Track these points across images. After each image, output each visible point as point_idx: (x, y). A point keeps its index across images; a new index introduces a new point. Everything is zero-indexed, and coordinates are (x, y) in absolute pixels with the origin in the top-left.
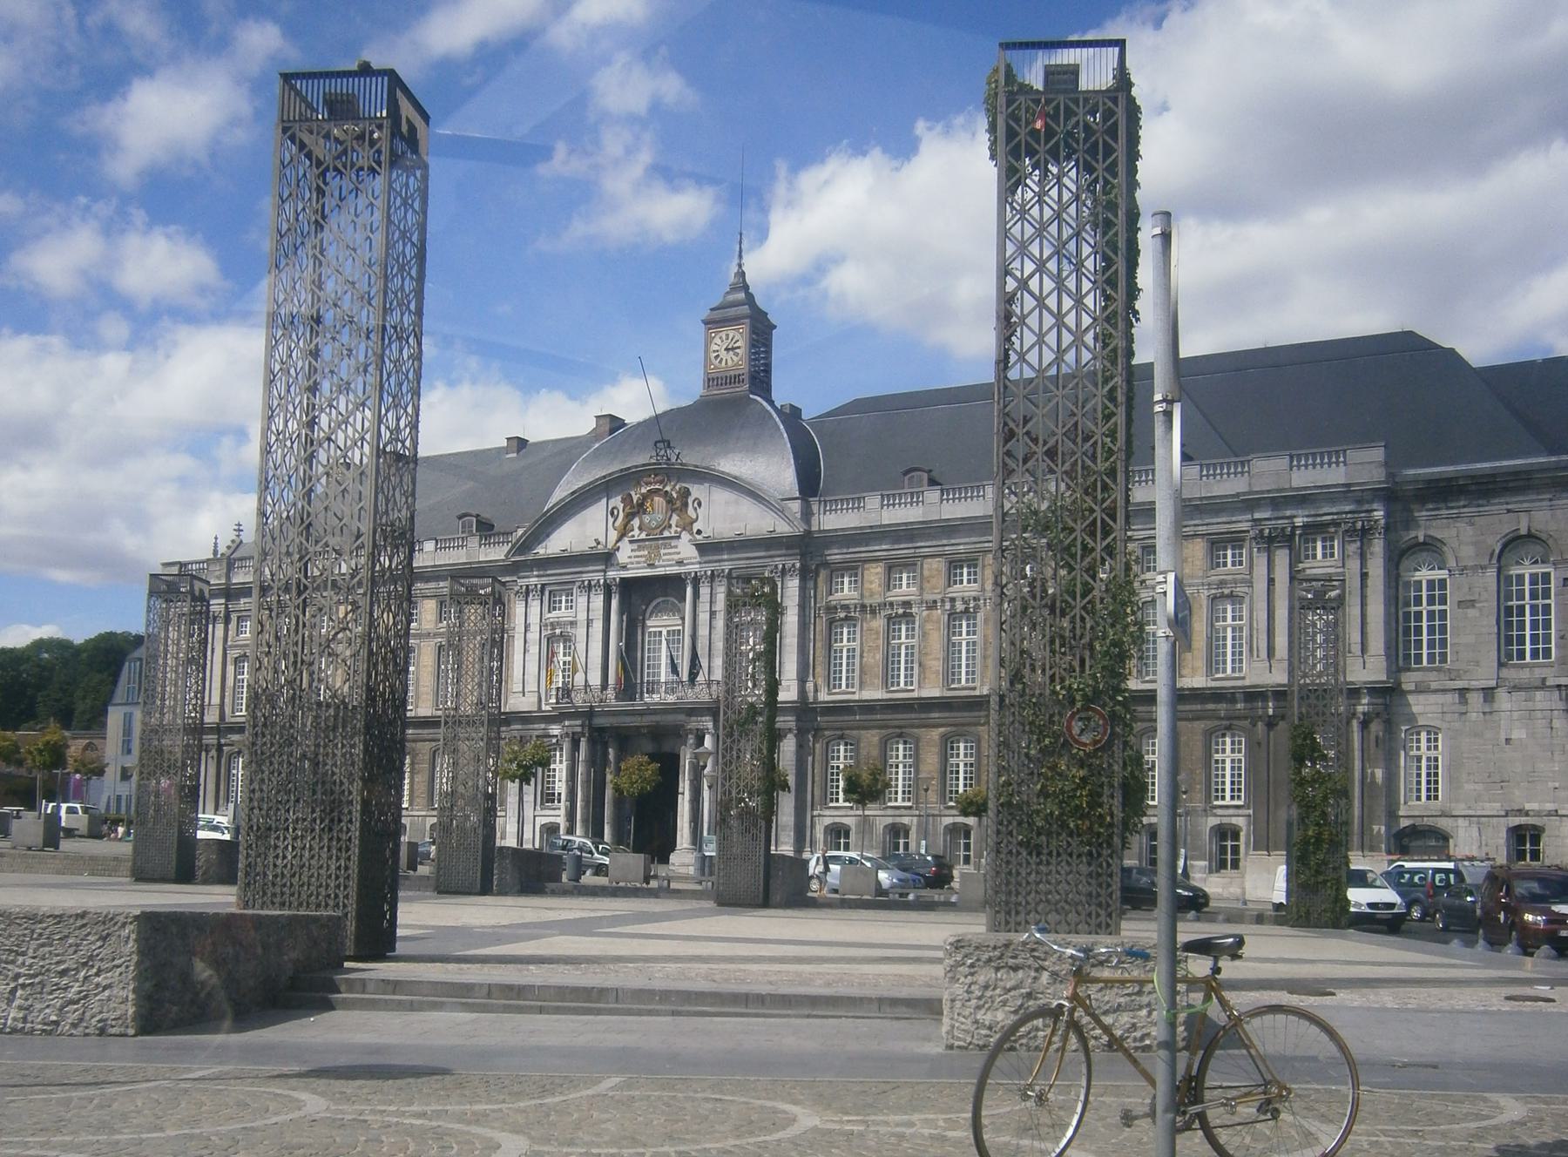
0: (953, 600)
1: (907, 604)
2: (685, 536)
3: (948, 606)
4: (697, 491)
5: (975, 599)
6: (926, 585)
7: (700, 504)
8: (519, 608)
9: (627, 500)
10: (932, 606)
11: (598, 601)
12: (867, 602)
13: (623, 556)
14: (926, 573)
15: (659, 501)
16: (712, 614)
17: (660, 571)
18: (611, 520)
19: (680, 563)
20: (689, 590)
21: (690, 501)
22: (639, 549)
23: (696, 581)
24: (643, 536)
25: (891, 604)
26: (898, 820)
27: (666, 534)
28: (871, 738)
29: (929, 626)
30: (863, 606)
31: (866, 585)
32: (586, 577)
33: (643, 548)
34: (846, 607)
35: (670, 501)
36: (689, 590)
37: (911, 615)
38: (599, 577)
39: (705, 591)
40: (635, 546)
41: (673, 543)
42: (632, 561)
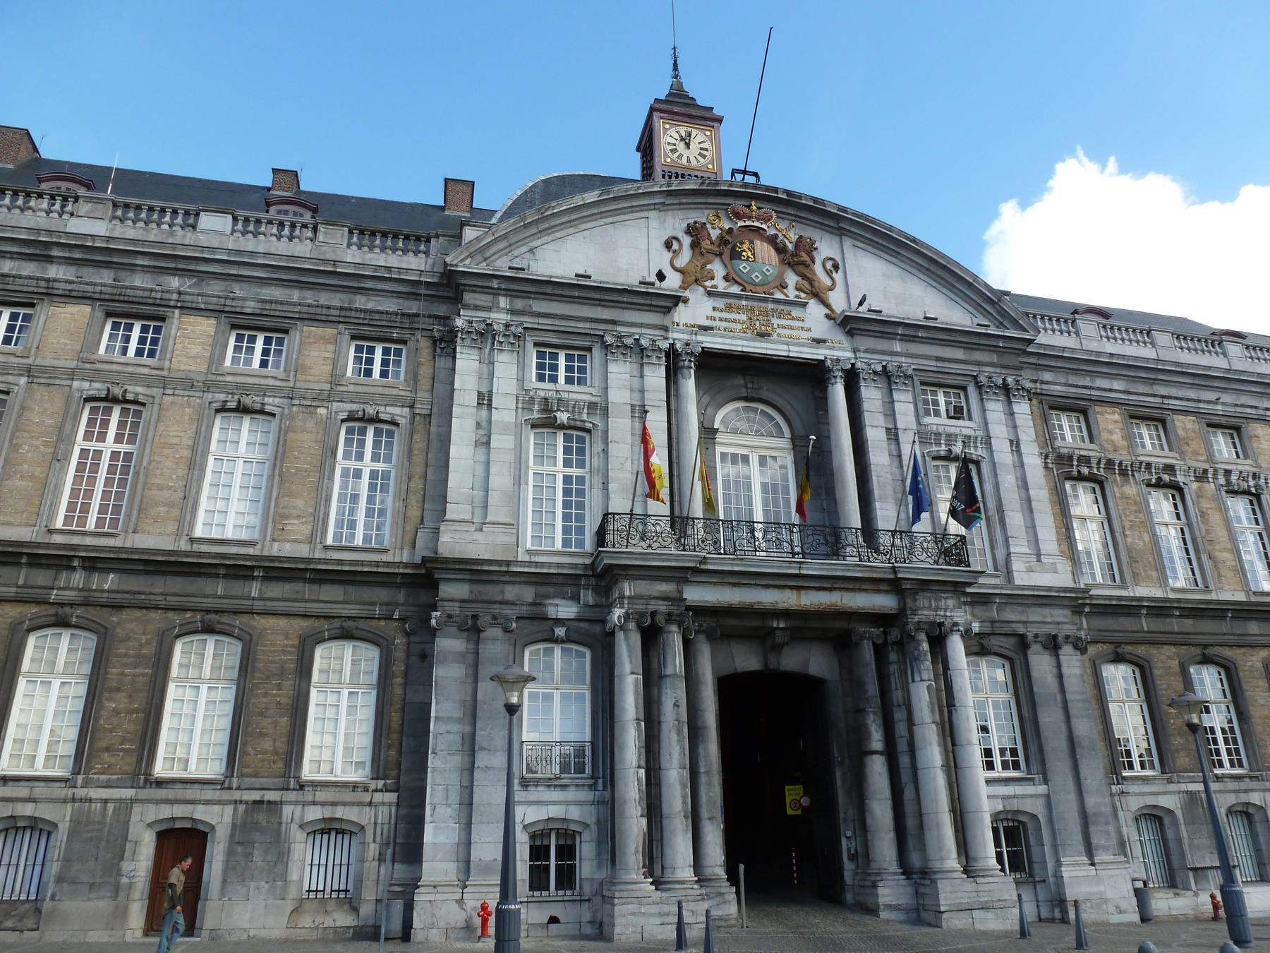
0: (1228, 473)
1: (1170, 469)
2: (815, 311)
3: (1222, 481)
4: (826, 247)
5: (1255, 476)
6: (1185, 448)
7: (836, 267)
8: (467, 362)
9: (695, 232)
10: (1201, 477)
11: (656, 377)
12: (1117, 458)
13: (697, 309)
14: (1181, 432)
18: (668, 256)
19: (818, 342)
20: (838, 392)
22: (729, 308)
23: (852, 379)
24: (735, 289)
25: (1149, 465)
27: (779, 295)
29: (1205, 504)
30: (1110, 463)
31: (1105, 435)
33: (739, 309)
34: (1085, 460)
35: (780, 250)
36: (838, 392)
37: (1177, 488)
39: (871, 396)
40: (720, 303)
41: (796, 312)
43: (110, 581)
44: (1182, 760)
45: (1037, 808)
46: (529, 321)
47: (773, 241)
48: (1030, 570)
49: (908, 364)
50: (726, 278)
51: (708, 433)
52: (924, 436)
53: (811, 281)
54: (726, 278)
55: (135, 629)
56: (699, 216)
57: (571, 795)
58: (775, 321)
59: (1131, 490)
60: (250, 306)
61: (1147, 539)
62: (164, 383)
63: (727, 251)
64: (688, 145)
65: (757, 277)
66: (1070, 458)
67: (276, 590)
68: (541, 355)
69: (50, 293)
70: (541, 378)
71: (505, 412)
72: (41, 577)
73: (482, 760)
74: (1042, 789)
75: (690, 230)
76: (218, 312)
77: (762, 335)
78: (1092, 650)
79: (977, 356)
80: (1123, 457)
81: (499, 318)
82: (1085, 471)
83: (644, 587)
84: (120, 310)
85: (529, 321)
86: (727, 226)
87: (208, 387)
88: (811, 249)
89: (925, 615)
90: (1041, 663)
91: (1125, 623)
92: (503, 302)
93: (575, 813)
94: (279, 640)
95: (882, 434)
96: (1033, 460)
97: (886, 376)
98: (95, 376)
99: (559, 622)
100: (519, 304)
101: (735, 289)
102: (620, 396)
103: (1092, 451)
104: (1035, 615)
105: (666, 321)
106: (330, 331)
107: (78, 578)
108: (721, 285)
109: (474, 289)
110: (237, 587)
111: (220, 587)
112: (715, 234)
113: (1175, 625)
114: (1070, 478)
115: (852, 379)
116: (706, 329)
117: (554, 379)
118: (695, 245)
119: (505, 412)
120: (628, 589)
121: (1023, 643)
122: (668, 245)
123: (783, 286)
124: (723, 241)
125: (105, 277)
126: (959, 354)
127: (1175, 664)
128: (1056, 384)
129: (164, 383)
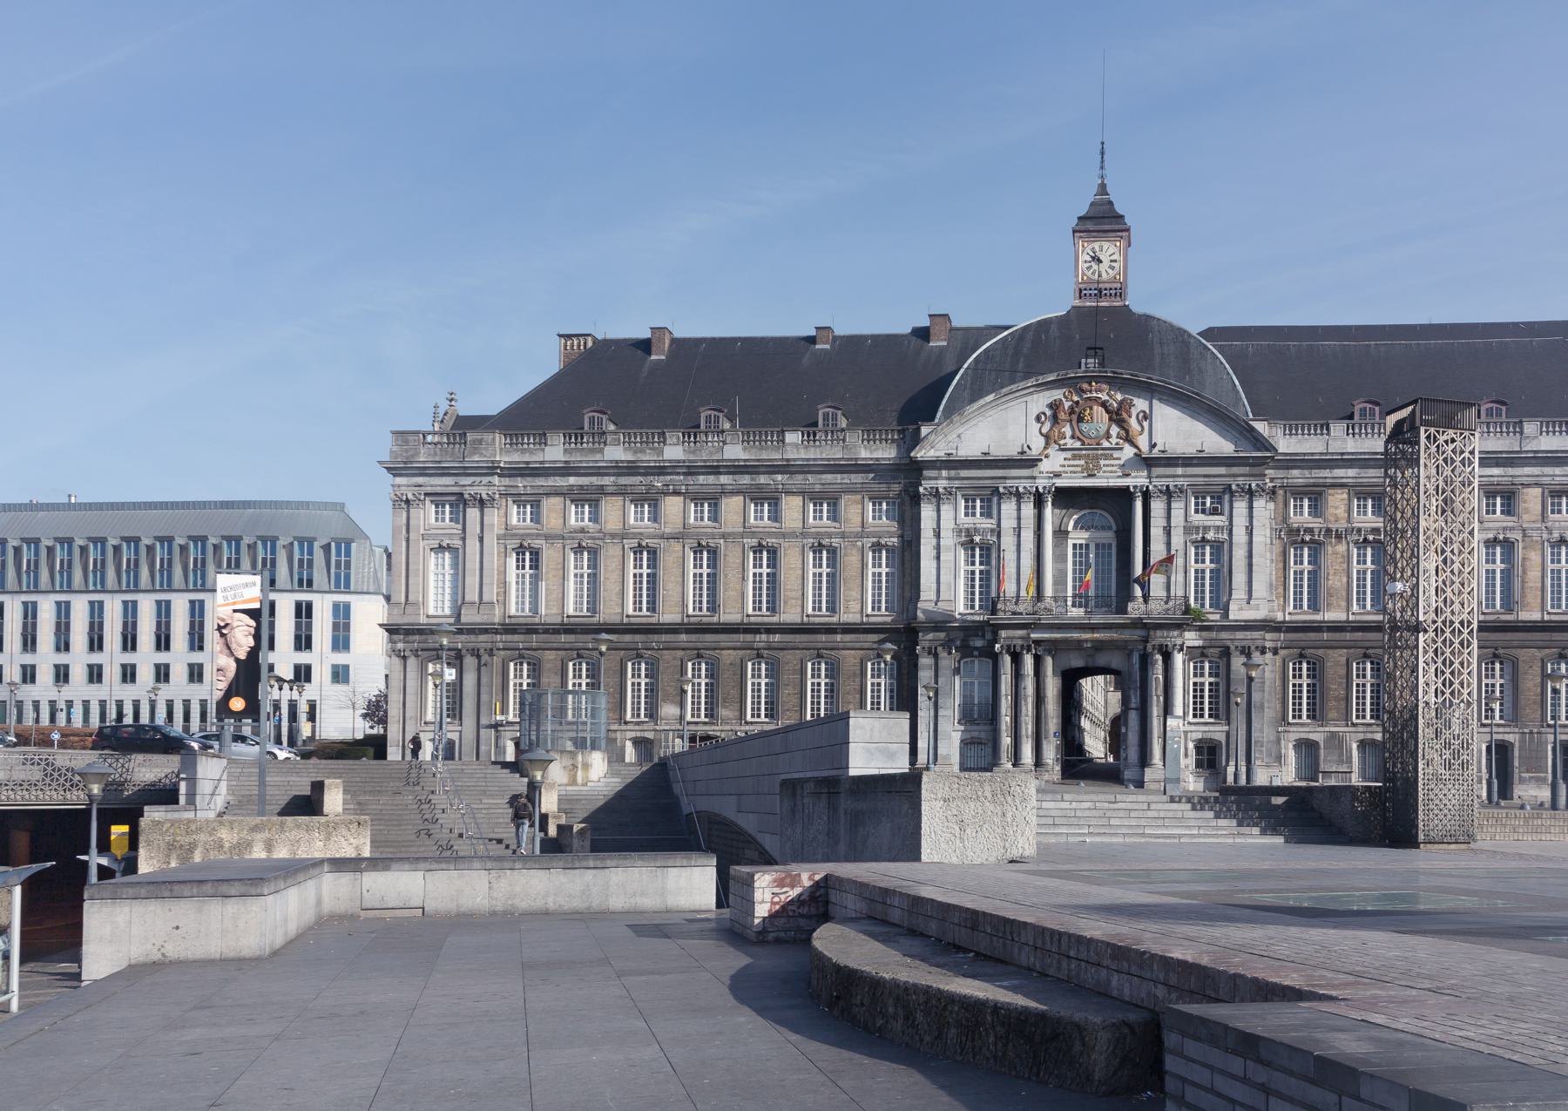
2: (1129, 452)
8: (927, 512)
9: (1055, 406)
11: (1028, 509)
12: (1333, 526)
13: (1054, 461)
15: (1098, 410)
16: (1168, 531)
17: (1098, 482)
21: (1134, 412)
22: (1075, 457)
23: (1147, 496)
24: (1078, 444)
25: (1359, 530)
26: (1369, 736)
27: (1106, 444)
28: (1339, 656)
30: (1329, 530)
31: (1331, 510)
32: (1009, 483)
34: (1310, 531)
38: (1022, 485)
39: (1157, 506)
40: (1069, 454)
42: (1059, 469)
43: (777, 637)
44: (1333, 714)
45: (1222, 738)
46: (957, 483)
47: (1104, 404)
48: (1241, 609)
49: (1181, 482)
50: (1073, 437)
51: (1060, 534)
52: (1189, 529)
53: (1127, 432)
54: (1073, 437)
55: (790, 658)
56: (1057, 394)
57: (981, 727)
58: (1102, 462)
59: (1342, 548)
60: (818, 488)
61: (1345, 580)
62: (784, 536)
63: (1075, 417)
64: (1100, 261)
65: (1093, 433)
66: (1298, 530)
67: (848, 637)
68: (967, 501)
69: (725, 492)
70: (966, 514)
71: (948, 539)
72: (749, 637)
73: (941, 712)
74: (1226, 728)
75: (1050, 406)
76: (802, 493)
77: (1091, 476)
78: (1282, 652)
79: (1235, 470)
80: (1342, 525)
81: (942, 484)
82: (1307, 538)
83: (1011, 633)
84: (758, 496)
85: (957, 483)
86: (1076, 398)
87: (804, 535)
88: (1131, 405)
89: (1157, 642)
90: (1238, 662)
91: (1312, 636)
92: (944, 473)
93: (983, 735)
94: (852, 661)
95: (1161, 531)
96: (1262, 536)
97: (1168, 494)
98: (753, 534)
99: (976, 648)
100: (953, 473)
101: (1078, 444)
102: (1008, 523)
103: (1316, 523)
104: (1240, 635)
105: (1034, 472)
106: (859, 497)
107: (764, 637)
108: (1070, 443)
109: (928, 468)
110: (831, 637)
111: (824, 637)
112: (1067, 405)
113: (1348, 636)
114: (1294, 542)
115: (1147, 496)
116: (1057, 475)
117: (974, 514)
118: (1055, 419)
119: (948, 539)
120: (1003, 634)
121: (1226, 653)
122: (1038, 419)
123: (1108, 436)
124: (1072, 411)
125: (746, 480)
126: (1222, 470)
127: (1344, 660)
128: (1297, 476)
129: (784, 536)
